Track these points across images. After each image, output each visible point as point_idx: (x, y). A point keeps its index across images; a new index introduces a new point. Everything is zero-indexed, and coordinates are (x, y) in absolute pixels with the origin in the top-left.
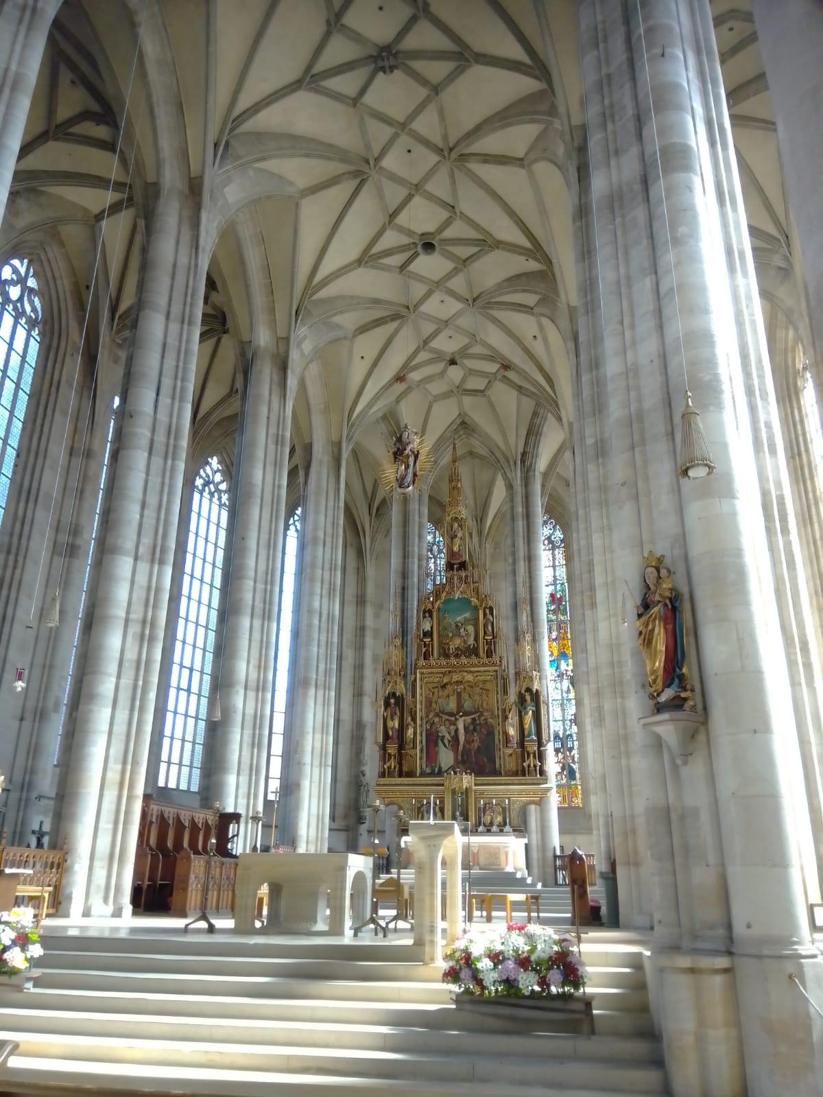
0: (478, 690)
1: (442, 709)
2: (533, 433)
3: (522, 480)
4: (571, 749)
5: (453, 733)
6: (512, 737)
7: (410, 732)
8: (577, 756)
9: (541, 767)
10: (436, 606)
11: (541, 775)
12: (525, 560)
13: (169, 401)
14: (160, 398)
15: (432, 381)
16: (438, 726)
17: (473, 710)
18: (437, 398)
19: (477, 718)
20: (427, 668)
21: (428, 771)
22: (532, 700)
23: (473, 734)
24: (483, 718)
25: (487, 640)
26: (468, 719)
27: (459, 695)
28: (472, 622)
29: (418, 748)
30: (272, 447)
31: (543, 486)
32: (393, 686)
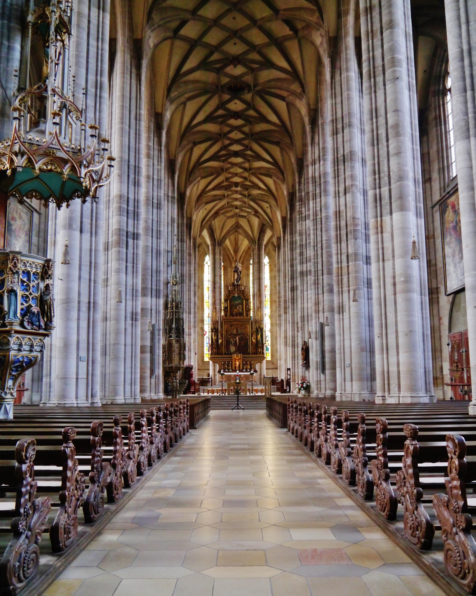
0: (243, 327)
2: (262, 231)
4: (268, 341)
7: (220, 341)
8: (270, 344)
18: (228, 218)
21: (227, 353)
26: (240, 336)
30: (188, 257)
31: (265, 250)
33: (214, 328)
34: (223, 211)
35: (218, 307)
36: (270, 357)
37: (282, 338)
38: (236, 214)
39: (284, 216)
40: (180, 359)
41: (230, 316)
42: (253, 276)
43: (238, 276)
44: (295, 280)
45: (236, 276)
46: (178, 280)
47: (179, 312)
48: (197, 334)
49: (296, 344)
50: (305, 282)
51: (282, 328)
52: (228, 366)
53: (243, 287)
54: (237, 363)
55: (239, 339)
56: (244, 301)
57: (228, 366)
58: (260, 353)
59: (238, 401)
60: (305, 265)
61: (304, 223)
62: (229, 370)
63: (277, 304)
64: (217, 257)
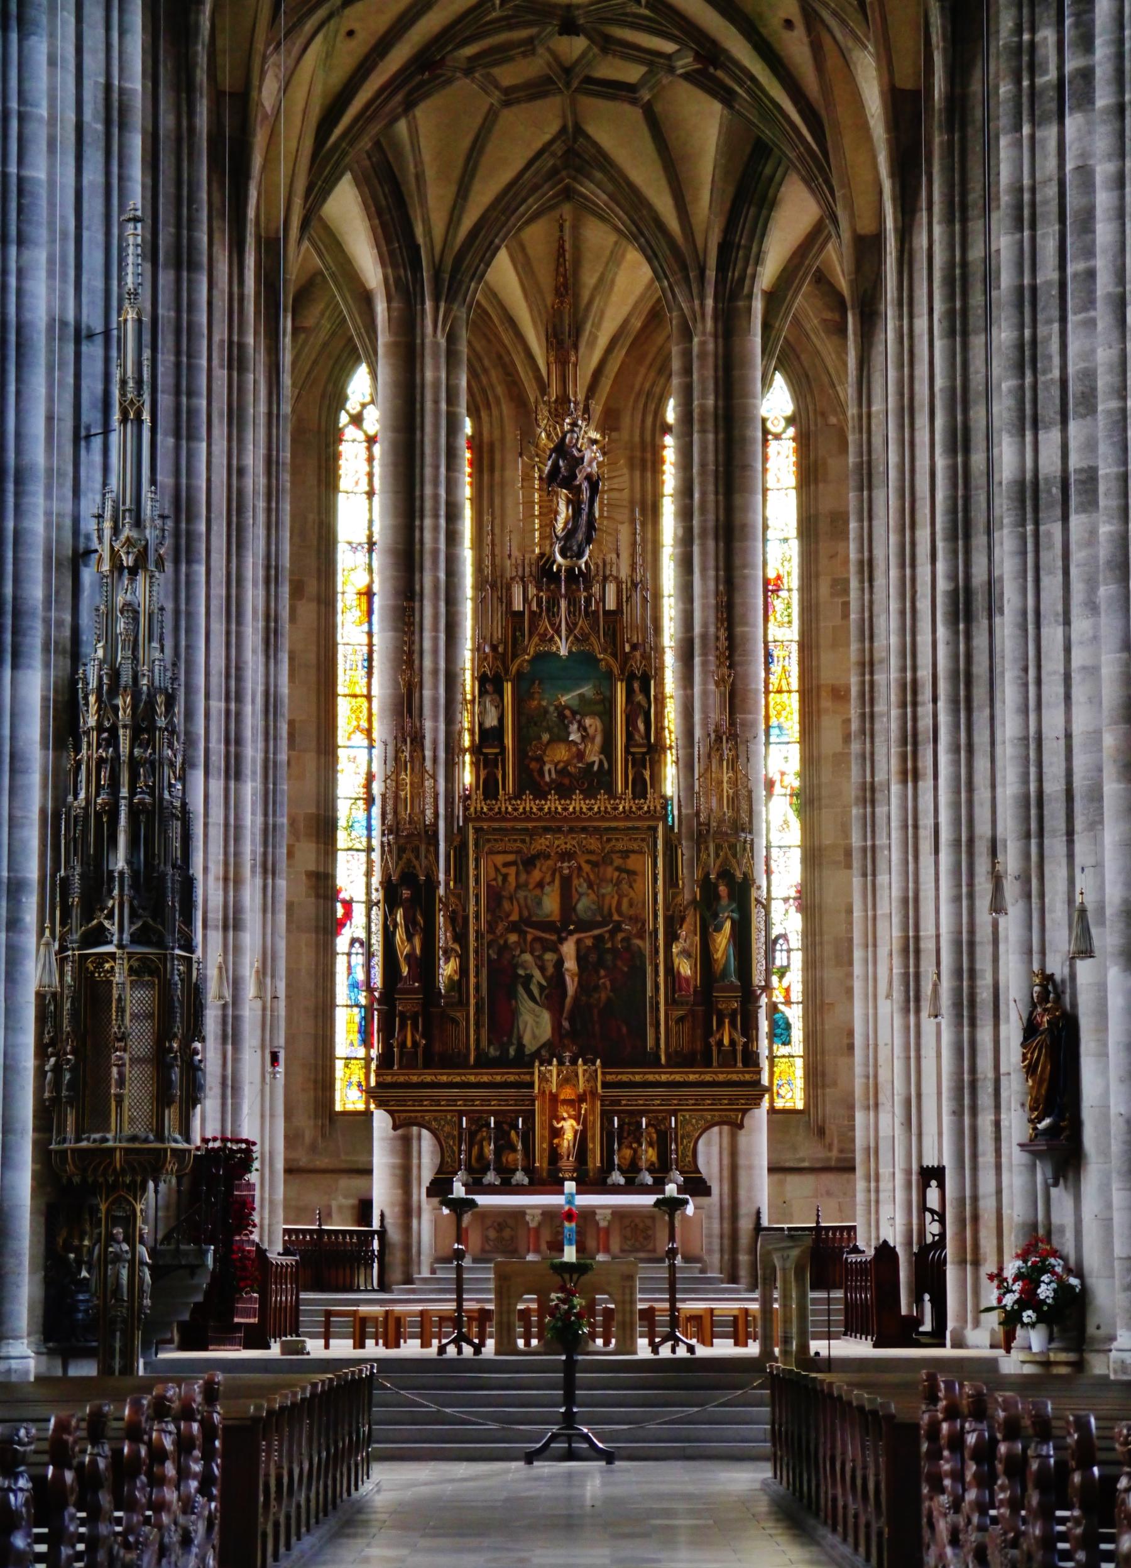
0: (610, 872)
1: (526, 913)
3: (716, 318)
4: (783, 972)
5: (550, 970)
6: (687, 980)
7: (447, 969)
8: (797, 994)
9: (746, 1045)
10: (514, 669)
11: (745, 1064)
13: (171, 441)
14: (159, 437)
15: (511, 59)
16: (517, 952)
17: (599, 919)
18: (512, 97)
19: (607, 936)
20: (491, 819)
21: (493, 1052)
22: (731, 896)
23: (597, 972)
24: (620, 936)
25: (633, 754)
27: (566, 882)
28: (600, 708)
29: (472, 1001)
30: (221, 375)
31: (767, 326)
32: (409, 861)
33: (408, 877)
34: (469, 51)
35: (433, 728)
36: (799, 1083)
37: (883, 951)
38: (568, 71)
39: (906, 83)
40: (162, 1098)
41: (518, 796)
42: (685, 514)
43: (577, 512)
44: (979, 540)
45: (564, 512)
46: (150, 534)
47: (154, 766)
48: (282, 918)
49: (984, 995)
50: (1051, 557)
51: (882, 879)
52: (504, 1146)
53: (611, 589)
54: (569, 1127)
55: (580, 959)
56: (620, 690)
57: (504, 1146)
58: (728, 1059)
59: (569, 1400)
60: (1050, 439)
61: (1050, 134)
62: (506, 1172)
63: (854, 712)
64: (429, 375)
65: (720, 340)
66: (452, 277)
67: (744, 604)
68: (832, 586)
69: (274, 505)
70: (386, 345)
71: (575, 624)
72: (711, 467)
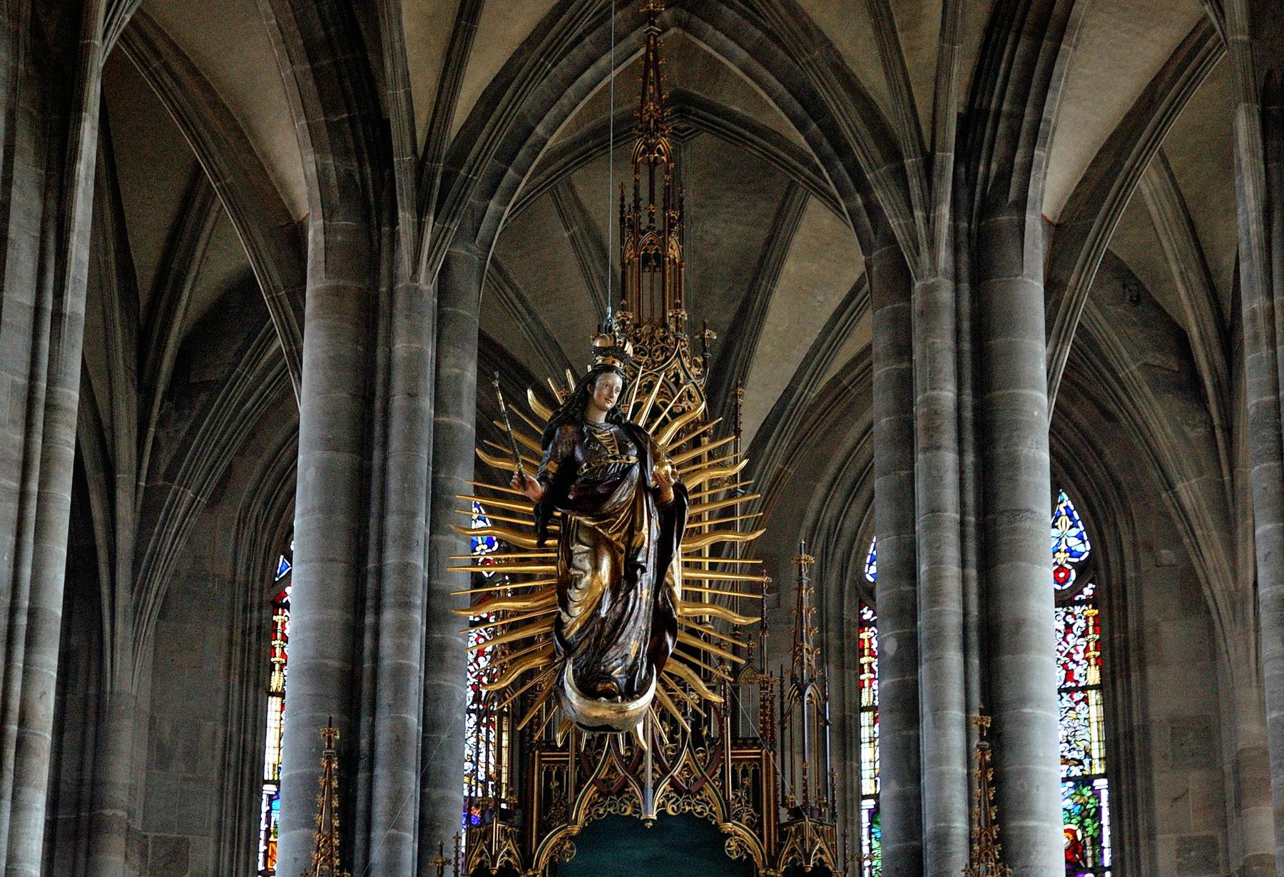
3: (956, 249)
12: (965, 649)
31: (1053, 286)
65: (965, 286)
66: (447, 177)
67: (1024, 773)
68: (1179, 853)
69: (34, 487)
70: (317, 295)
71: (676, 759)
72: (952, 514)
